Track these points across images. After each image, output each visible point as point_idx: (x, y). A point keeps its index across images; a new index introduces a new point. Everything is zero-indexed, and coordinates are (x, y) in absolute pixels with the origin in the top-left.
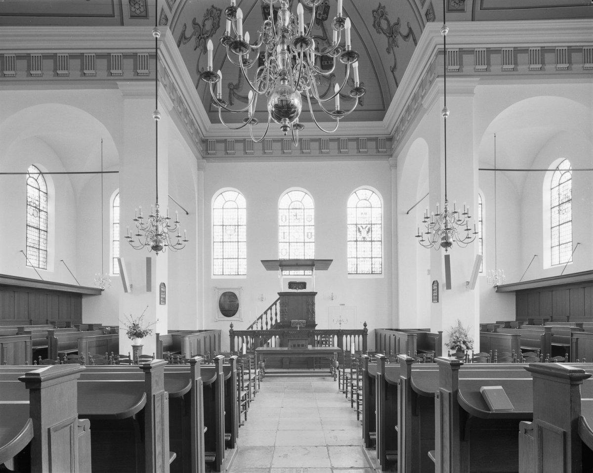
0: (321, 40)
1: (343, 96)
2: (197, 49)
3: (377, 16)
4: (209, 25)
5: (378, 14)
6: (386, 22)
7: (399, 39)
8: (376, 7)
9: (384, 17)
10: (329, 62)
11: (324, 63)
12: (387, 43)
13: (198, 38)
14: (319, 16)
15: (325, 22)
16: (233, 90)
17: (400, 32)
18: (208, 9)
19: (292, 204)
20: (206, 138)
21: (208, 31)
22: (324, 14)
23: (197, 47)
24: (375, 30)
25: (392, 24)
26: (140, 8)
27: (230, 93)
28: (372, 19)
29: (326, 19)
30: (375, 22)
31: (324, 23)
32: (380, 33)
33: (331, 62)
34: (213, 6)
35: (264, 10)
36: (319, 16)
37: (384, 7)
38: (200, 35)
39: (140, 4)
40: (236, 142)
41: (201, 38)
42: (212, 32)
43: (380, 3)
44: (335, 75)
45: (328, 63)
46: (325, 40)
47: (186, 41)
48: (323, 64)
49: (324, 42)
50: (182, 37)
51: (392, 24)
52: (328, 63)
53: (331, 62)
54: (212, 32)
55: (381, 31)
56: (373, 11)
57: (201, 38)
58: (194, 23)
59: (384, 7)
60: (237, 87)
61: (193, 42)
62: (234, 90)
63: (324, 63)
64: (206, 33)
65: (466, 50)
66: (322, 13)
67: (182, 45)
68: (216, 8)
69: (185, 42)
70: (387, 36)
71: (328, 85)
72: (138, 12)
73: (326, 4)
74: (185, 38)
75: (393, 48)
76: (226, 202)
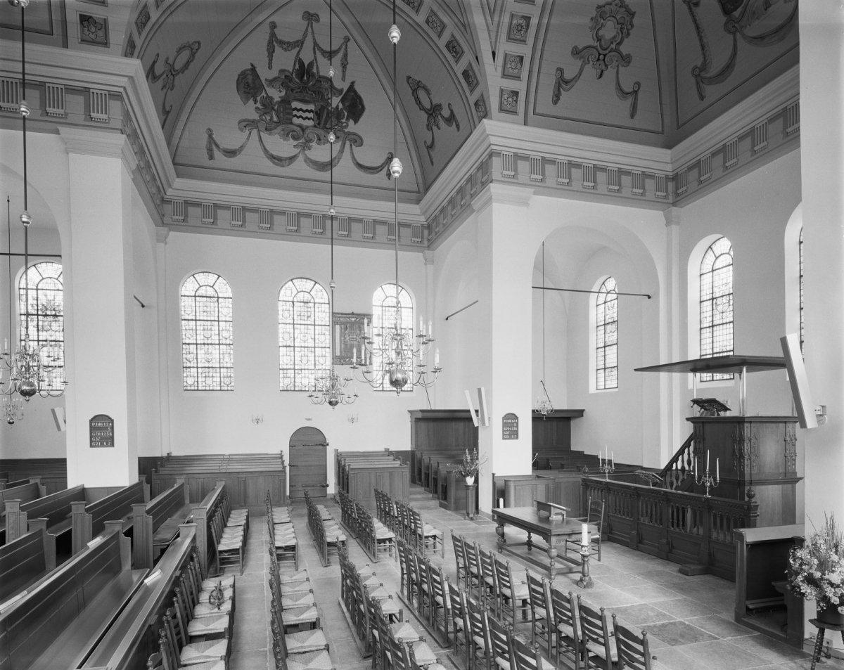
2: (605, 73)
4: (609, 30)
13: (598, 60)
18: (592, 19)
20: (674, 172)
21: (614, 37)
23: (602, 71)
27: (697, 83)
34: (599, 7)
38: (600, 54)
41: (605, 55)
42: (625, 31)
47: (572, 83)
50: (559, 85)
54: (625, 31)
58: (576, 52)
61: (590, 71)
64: (612, 43)
67: (564, 95)
69: (568, 87)
74: (566, 82)
76: (717, 258)
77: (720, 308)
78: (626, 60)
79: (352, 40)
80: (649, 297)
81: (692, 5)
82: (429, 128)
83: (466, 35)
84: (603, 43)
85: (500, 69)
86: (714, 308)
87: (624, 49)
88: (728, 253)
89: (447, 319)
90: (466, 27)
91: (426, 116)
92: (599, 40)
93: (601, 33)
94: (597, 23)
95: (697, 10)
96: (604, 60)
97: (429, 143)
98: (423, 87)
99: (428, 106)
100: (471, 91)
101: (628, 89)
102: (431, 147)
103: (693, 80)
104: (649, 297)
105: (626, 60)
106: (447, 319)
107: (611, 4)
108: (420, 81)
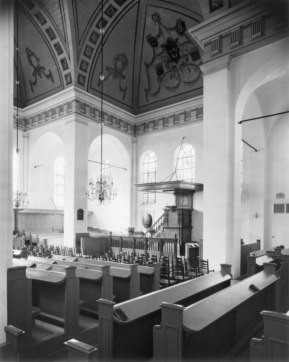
0: (188, 44)
4: (119, 64)
14: (181, 30)
16: (147, 92)
18: (114, 58)
19: (185, 154)
22: (182, 28)
36: (181, 30)
38: (115, 72)
40: (159, 121)
46: (190, 43)
57: (117, 73)
60: (149, 89)
62: (148, 92)
66: (181, 28)
68: (120, 55)
73: (181, 21)
76: (150, 159)
77: (151, 177)
78: (124, 77)
80: (126, 170)
81: (147, 67)
82: (34, 74)
84: (117, 68)
85: (79, 67)
86: (149, 176)
87: (124, 73)
88: (154, 158)
89: (35, 167)
91: (34, 69)
92: (116, 67)
93: (117, 64)
94: (116, 60)
96: (116, 75)
97: (33, 81)
98: (36, 57)
99: (36, 65)
101: (123, 88)
102: (35, 83)
103: (144, 93)
104: (126, 170)
105: (124, 77)
106: (35, 167)
107: (121, 55)
108: (34, 53)
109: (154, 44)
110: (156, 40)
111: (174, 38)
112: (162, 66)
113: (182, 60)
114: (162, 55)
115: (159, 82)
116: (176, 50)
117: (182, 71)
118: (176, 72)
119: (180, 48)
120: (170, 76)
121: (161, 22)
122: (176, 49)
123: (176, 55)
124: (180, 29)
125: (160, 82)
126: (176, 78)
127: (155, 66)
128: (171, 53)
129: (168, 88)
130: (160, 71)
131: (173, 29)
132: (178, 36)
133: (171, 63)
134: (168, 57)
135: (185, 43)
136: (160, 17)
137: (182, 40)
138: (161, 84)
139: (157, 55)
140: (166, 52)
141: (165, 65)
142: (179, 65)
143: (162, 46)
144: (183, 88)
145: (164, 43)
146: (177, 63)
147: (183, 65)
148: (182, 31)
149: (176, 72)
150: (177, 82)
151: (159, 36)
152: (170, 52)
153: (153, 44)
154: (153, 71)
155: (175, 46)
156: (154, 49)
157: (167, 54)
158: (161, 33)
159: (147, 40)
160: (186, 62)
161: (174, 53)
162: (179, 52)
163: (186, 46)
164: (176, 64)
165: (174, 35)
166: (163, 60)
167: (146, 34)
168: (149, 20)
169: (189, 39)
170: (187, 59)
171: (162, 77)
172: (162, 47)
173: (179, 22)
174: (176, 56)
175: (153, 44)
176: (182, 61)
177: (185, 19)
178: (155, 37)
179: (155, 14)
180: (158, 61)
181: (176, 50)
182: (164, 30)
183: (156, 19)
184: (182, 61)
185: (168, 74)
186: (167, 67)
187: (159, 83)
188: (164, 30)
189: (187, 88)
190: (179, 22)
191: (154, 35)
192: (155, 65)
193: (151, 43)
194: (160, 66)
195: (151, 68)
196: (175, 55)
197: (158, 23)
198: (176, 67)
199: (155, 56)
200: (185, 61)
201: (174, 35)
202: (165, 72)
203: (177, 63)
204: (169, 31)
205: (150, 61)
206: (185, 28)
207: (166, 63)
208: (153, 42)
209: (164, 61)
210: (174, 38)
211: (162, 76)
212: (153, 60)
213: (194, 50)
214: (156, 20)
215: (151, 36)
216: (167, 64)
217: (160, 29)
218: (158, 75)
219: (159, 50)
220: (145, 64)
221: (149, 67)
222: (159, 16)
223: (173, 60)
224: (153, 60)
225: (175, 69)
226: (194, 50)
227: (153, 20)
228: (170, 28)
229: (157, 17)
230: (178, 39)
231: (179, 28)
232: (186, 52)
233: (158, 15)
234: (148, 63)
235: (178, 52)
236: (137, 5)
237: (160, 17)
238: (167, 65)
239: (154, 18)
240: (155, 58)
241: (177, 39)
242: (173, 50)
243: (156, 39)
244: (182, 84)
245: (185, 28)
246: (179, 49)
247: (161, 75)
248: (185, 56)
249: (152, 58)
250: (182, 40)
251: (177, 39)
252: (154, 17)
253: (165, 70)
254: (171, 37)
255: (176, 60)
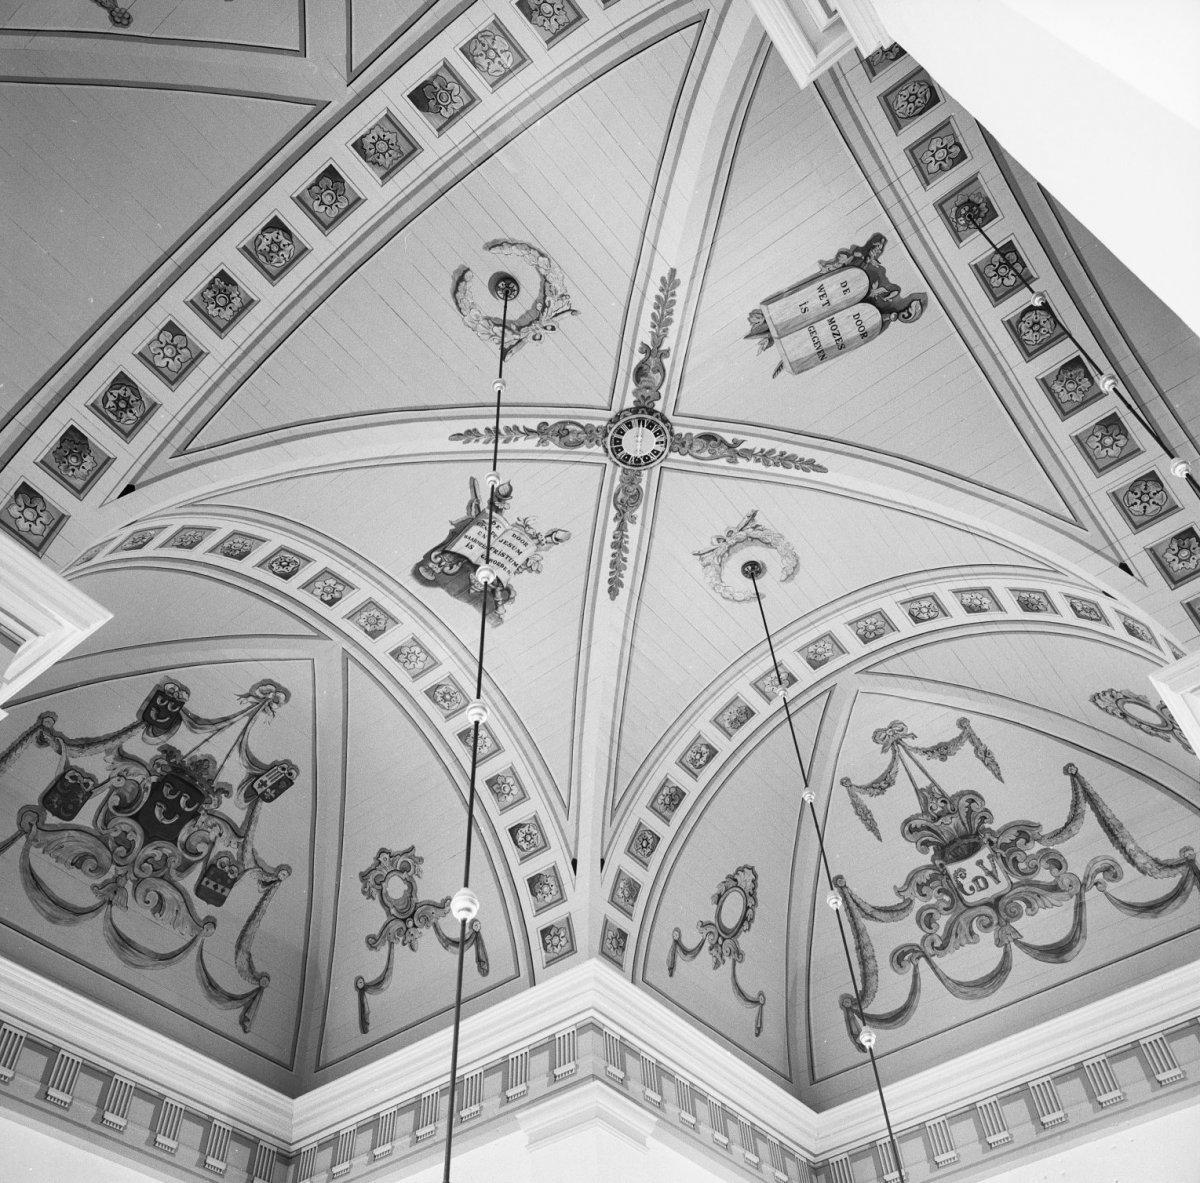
1: (210, 984)
3: (386, 863)
5: (392, 864)
6: (406, 887)
7: (426, 937)
8: (397, 847)
9: (405, 875)
10: (220, 887)
11: (207, 883)
12: (380, 926)
14: (260, 786)
15: (263, 806)
17: (435, 926)
22: (271, 788)
24: (361, 885)
25: (422, 896)
26: (34, 522)
28: (370, 862)
29: (270, 800)
30: (370, 871)
31: (259, 804)
32: (371, 896)
33: (223, 891)
35: (155, 697)
36: (260, 786)
37: (421, 860)
39: (39, 516)
43: (413, 848)
44: (217, 923)
45: (216, 887)
46: (240, 837)
48: (203, 883)
49: (235, 840)
51: (422, 896)
52: (216, 887)
53: (223, 891)
55: (377, 897)
56: (382, 851)
59: (421, 860)
63: (207, 883)
65: (630, 1046)
66: (269, 784)
70: (389, 913)
71: (190, 938)
72: (23, 525)
73: (290, 774)
75: (391, 945)
79: (107, 26)
83: (169, 450)
90: (186, 449)
95: (32, 745)
100: (44, 464)
109: (158, 716)
110: (176, 720)
111: (222, 778)
112: (91, 793)
113: (168, 851)
114: (133, 769)
115: (19, 824)
116: (187, 809)
117: (138, 881)
118: (112, 861)
119: (202, 818)
120: (82, 850)
121: (261, 715)
122: (188, 804)
123: (171, 819)
124: (264, 784)
125: (27, 828)
126: (99, 882)
127: (67, 762)
128: (165, 801)
129: (34, 883)
130: (65, 795)
131: (253, 762)
132: (235, 785)
133: (130, 821)
134: (139, 795)
135: (228, 822)
136: (274, 706)
137: (233, 808)
138: (22, 841)
139: (120, 749)
140: (154, 779)
141: (109, 796)
142: (149, 851)
143: (169, 752)
144: (88, 938)
145: (184, 753)
146: (148, 840)
147: (160, 869)
148: (259, 791)
149: (112, 861)
150: (90, 899)
151: (196, 722)
152: (166, 790)
153: (153, 714)
154: (39, 769)
155: (198, 797)
156: (133, 727)
157: (150, 785)
158: (214, 728)
159: (158, 686)
160: (173, 874)
161: (172, 809)
162: (190, 823)
163: (220, 835)
164: (139, 840)
165: (233, 773)
166: (114, 782)
167: (182, 676)
168: (249, 676)
169: (249, 827)
170: (185, 867)
171: (47, 822)
172: (164, 751)
173: (284, 769)
174: (166, 822)
175: (153, 714)
176: (165, 858)
177: (302, 781)
178: (186, 712)
179: (279, 688)
180: (96, 764)
181: (187, 809)
182: (232, 733)
183: (261, 696)
184: (165, 858)
185: (84, 837)
186: (101, 817)
187: (14, 829)
188: (232, 733)
189: (111, 961)
190: (284, 769)
191: (193, 706)
192: (73, 762)
193: (151, 702)
194: (87, 785)
195: (49, 752)
196: (167, 815)
197: (250, 705)
198: (129, 851)
199: (109, 745)
200: (175, 862)
201: (233, 773)
202: (78, 820)
203: (148, 840)
204: (236, 748)
205: (72, 735)
206: (273, 795)
207: (115, 800)
208: (164, 710)
209: (113, 789)
210: (222, 778)
211: (51, 819)
212: (86, 743)
213: (227, 869)
214: (257, 697)
215: (185, 695)
216: (116, 808)
217: (225, 719)
218: (46, 799)
219: (142, 746)
220: (41, 718)
221: (42, 742)
222: (277, 703)
223: (144, 818)
224: (86, 743)
225: (121, 850)
226: (227, 869)
227: (255, 687)
228: (249, 744)
229: (271, 696)
230: (227, 793)
231: (264, 778)
232: (203, 848)
233: (282, 696)
234: (58, 727)
235: (186, 817)
236: (308, 632)
237: (274, 706)
238: (108, 809)
239: (264, 688)
240: (101, 747)
241: (225, 791)
242: (179, 798)
243: (181, 720)
244: (98, 922)
245: (273, 795)
246: (195, 815)
247: (53, 815)
248: (190, 854)
249: (101, 733)
250: (233, 808)
251: (225, 791)
252: (270, 687)
253: (86, 816)
254: (218, 766)
255: (153, 832)
